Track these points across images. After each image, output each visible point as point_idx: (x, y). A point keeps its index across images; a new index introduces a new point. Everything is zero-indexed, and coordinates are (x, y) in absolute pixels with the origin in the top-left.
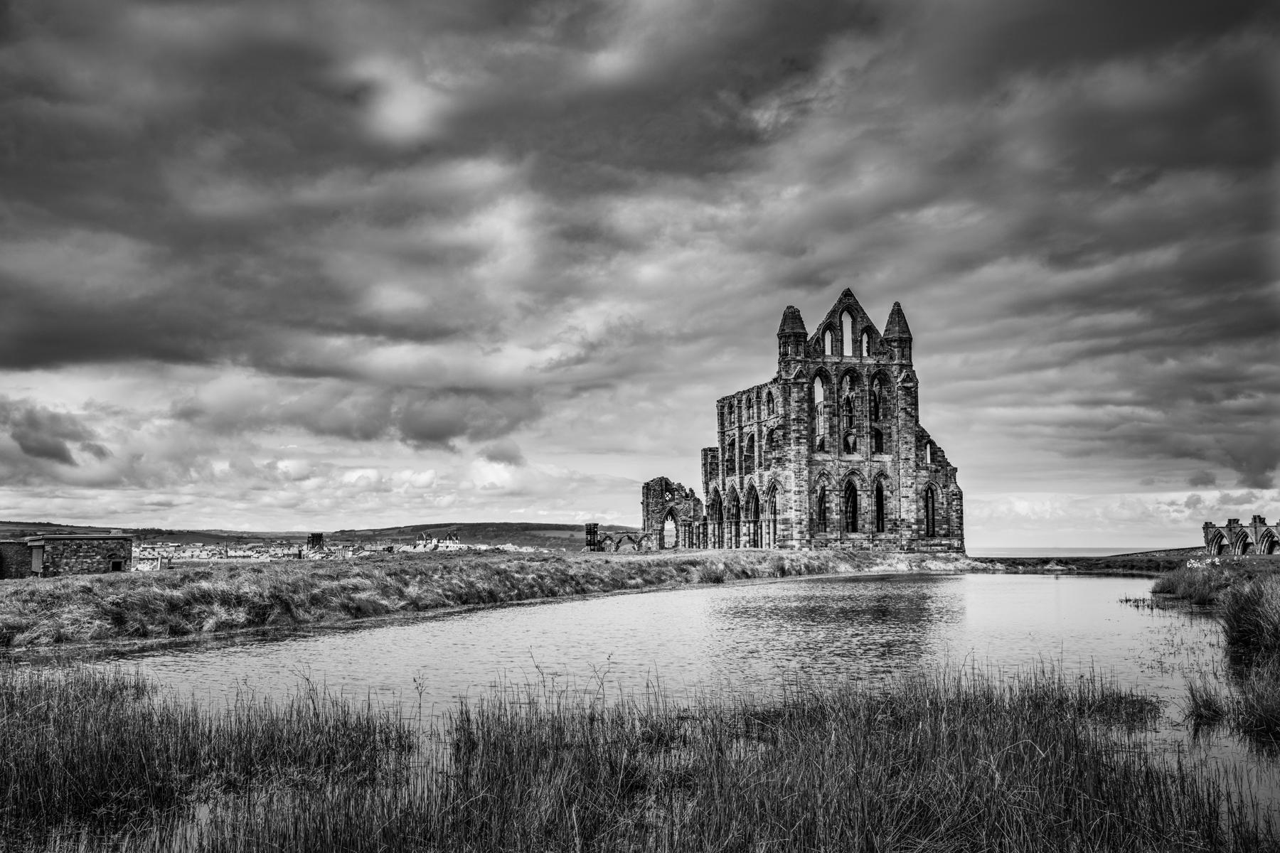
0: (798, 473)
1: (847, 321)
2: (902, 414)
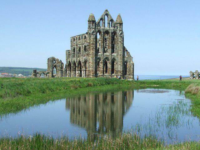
2: (120, 43)
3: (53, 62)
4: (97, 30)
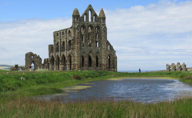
0: (77, 52)
1: (90, 12)
2: (103, 37)
3: (31, 58)
4: (81, 25)
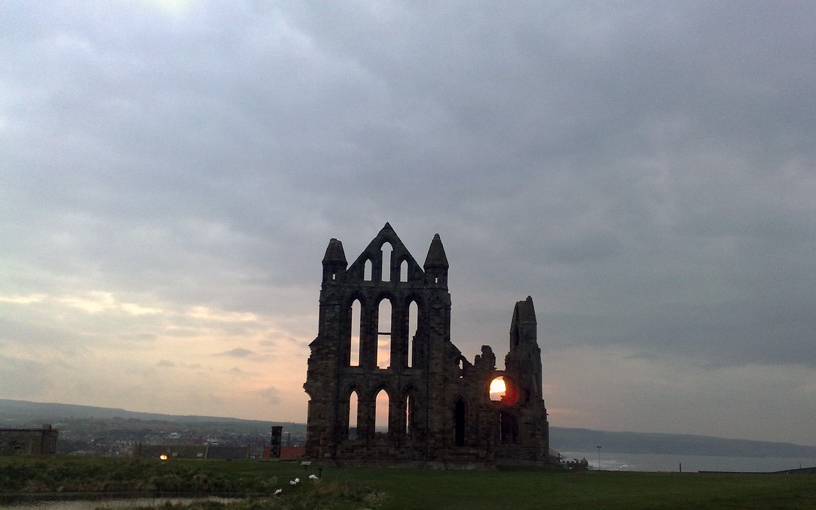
1: (387, 249)
